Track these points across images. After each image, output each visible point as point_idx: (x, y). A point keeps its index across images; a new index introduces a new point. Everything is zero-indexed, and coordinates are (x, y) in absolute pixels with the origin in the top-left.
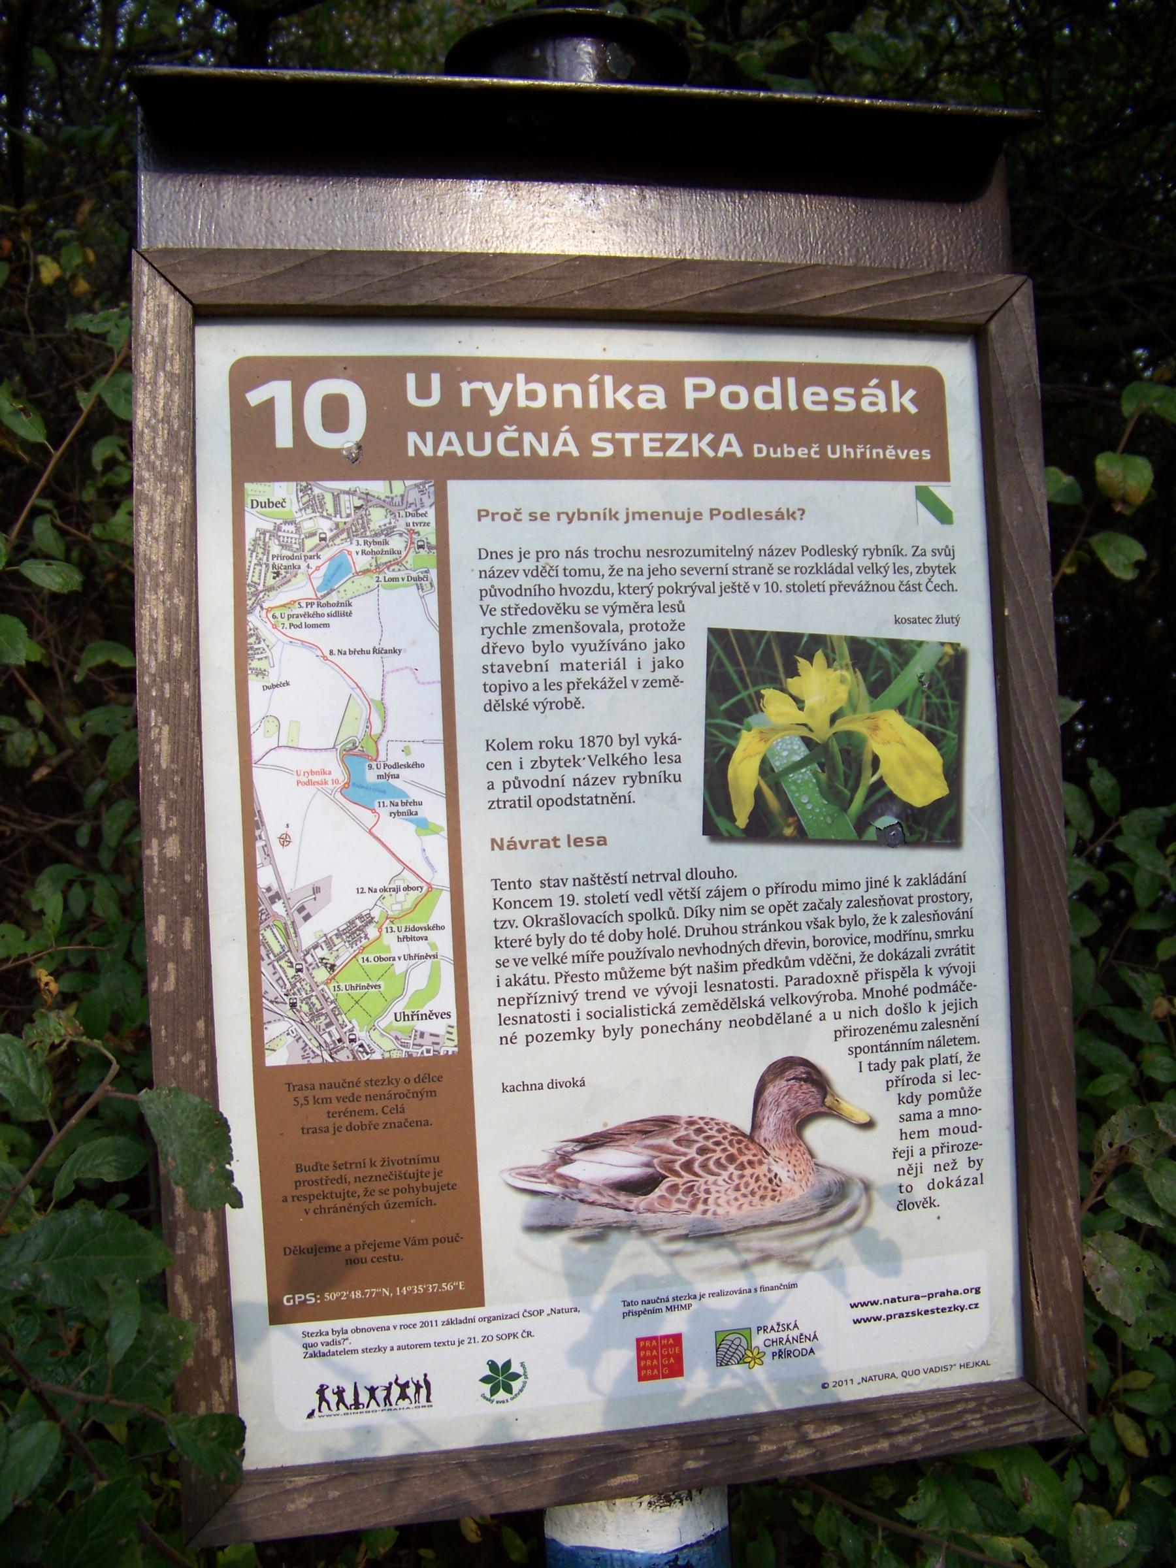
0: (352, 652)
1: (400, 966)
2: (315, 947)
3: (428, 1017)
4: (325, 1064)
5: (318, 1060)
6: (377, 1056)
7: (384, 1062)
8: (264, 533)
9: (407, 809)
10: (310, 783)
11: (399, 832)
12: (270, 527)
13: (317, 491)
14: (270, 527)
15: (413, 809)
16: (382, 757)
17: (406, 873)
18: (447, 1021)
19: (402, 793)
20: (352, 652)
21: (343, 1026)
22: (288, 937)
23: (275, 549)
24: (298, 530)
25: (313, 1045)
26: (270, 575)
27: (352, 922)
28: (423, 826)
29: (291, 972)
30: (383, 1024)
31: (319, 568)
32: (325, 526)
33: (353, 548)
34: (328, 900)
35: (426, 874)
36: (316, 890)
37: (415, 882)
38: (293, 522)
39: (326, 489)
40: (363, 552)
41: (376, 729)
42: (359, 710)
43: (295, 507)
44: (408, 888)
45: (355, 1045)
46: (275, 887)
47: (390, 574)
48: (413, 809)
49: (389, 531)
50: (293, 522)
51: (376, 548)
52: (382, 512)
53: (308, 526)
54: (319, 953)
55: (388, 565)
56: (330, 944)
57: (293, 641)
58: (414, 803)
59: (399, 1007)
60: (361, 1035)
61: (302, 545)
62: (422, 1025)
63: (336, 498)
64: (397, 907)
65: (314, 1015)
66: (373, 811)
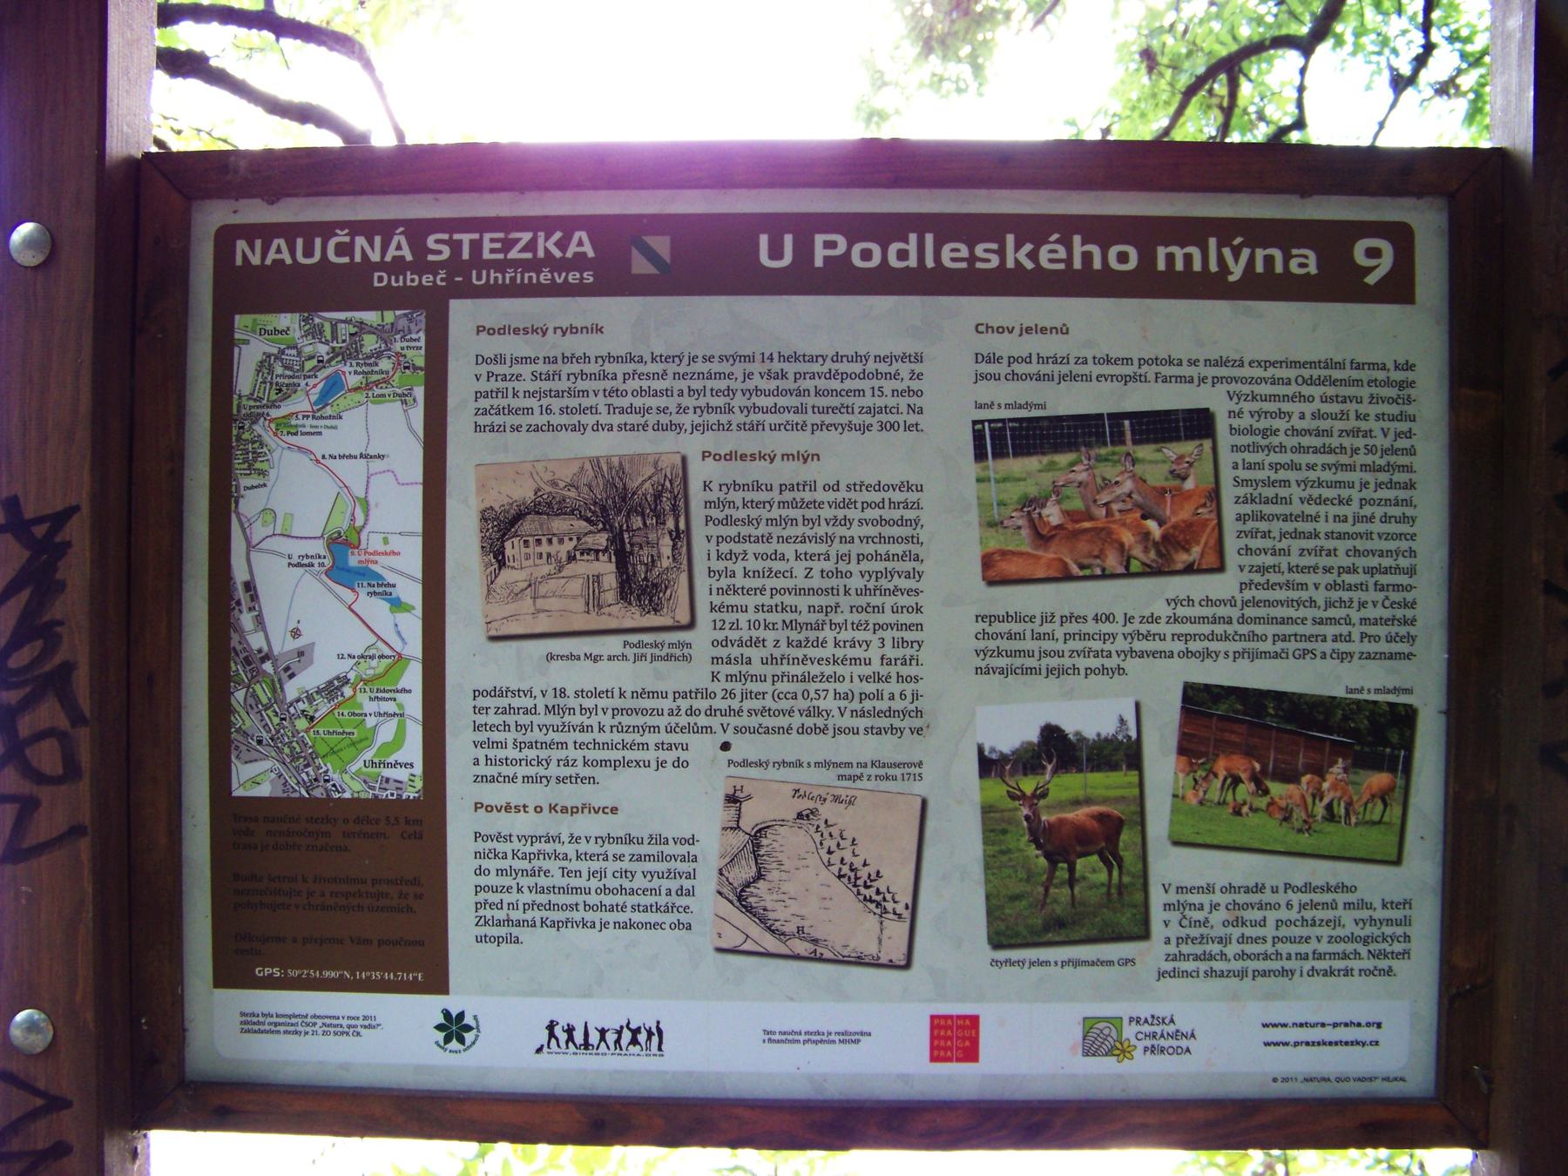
0: (342, 457)
1: (371, 722)
2: (298, 701)
3: (396, 764)
4: (302, 798)
5: (296, 795)
6: (347, 795)
7: (355, 801)
8: (269, 356)
9: (382, 589)
10: (299, 565)
11: (376, 609)
12: (275, 351)
13: (317, 321)
14: (275, 351)
15: (388, 590)
16: (363, 546)
17: (380, 644)
18: (409, 771)
19: (380, 577)
20: (342, 457)
21: (319, 768)
22: (274, 691)
23: (279, 370)
24: (299, 353)
25: (292, 782)
26: (273, 392)
27: (330, 683)
28: (397, 605)
29: (276, 720)
30: (354, 768)
31: (316, 386)
32: (323, 349)
33: (347, 369)
34: (311, 662)
35: (398, 646)
36: (301, 654)
37: (387, 652)
38: (295, 347)
39: (325, 319)
40: (356, 372)
41: (359, 522)
42: (346, 504)
43: (297, 334)
44: (382, 657)
45: (329, 785)
46: (266, 649)
47: (377, 391)
48: (388, 590)
49: (378, 355)
50: (295, 347)
51: (366, 369)
52: (372, 338)
53: (308, 350)
54: (301, 706)
55: (377, 383)
56: (310, 699)
57: (291, 447)
58: (389, 585)
59: (368, 755)
60: (335, 777)
61: (303, 366)
62: (387, 772)
63: (334, 325)
64: (371, 672)
65: (294, 758)
66: (353, 590)
